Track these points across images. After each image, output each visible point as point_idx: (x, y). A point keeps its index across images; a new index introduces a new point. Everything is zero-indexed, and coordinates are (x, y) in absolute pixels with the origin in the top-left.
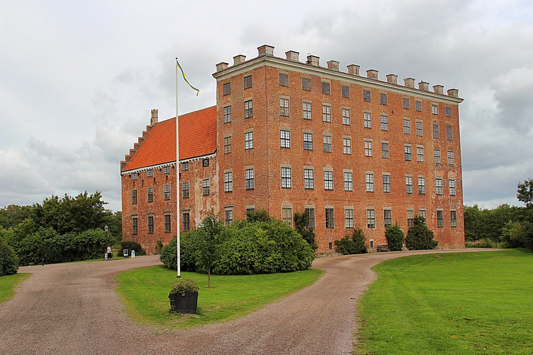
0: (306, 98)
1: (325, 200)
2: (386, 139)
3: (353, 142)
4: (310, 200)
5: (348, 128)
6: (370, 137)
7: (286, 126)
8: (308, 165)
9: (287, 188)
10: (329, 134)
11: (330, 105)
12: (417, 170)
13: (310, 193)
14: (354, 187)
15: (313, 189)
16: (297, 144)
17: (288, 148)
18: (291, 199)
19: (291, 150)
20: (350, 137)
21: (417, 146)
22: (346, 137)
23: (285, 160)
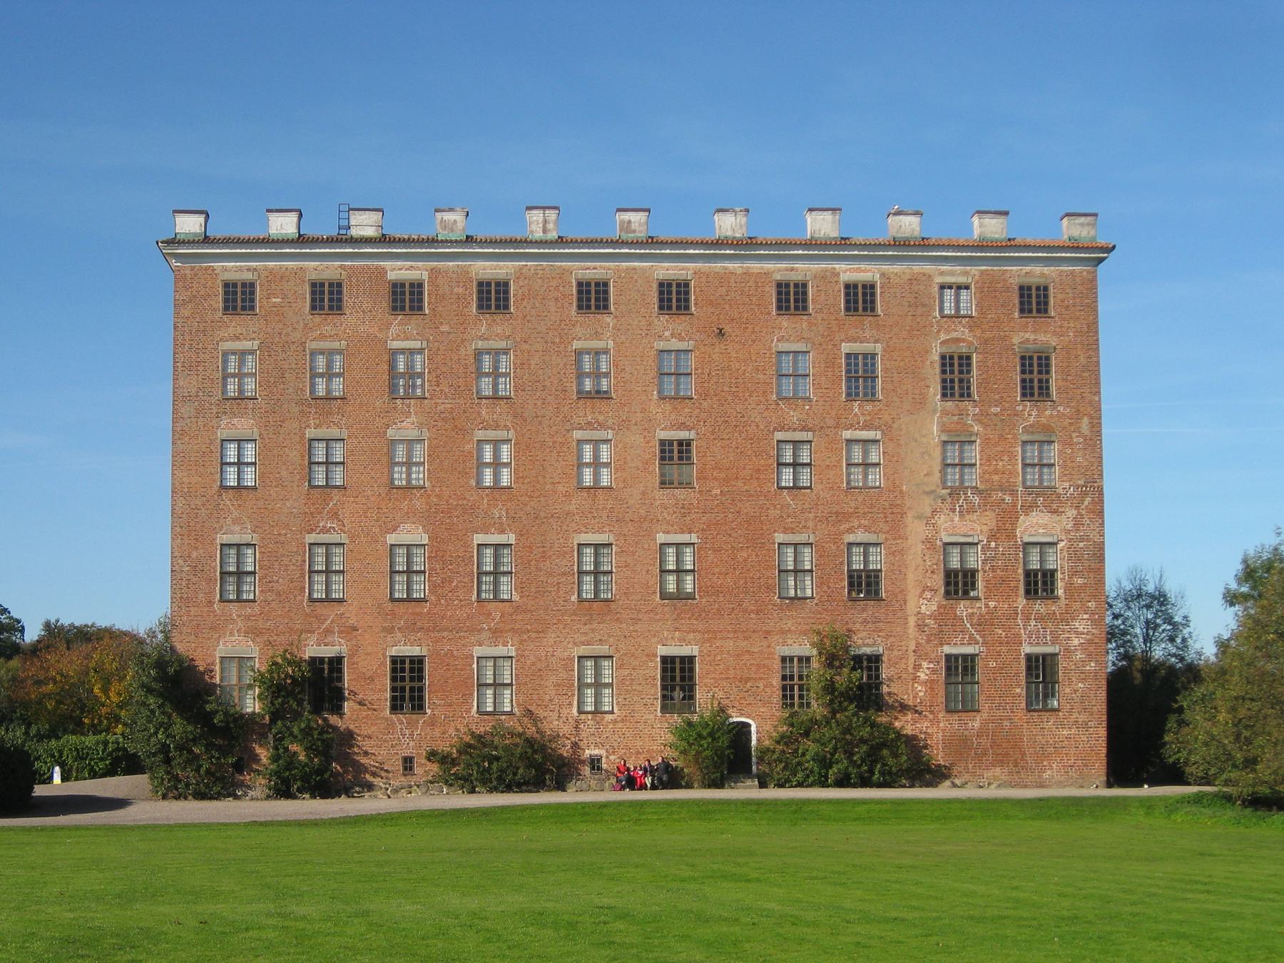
0: (322, 337)
1: (390, 630)
2: (683, 426)
3: (520, 449)
4: (328, 631)
5: (501, 407)
6: (602, 426)
7: (243, 425)
8: (326, 531)
9: (239, 600)
10: (413, 434)
11: (417, 344)
12: (842, 517)
13: (331, 612)
14: (521, 588)
15: (340, 601)
16: (284, 473)
17: (247, 488)
18: (253, 633)
19: (260, 493)
20: (511, 434)
21: (847, 434)
22: (491, 434)
23: (236, 521)
